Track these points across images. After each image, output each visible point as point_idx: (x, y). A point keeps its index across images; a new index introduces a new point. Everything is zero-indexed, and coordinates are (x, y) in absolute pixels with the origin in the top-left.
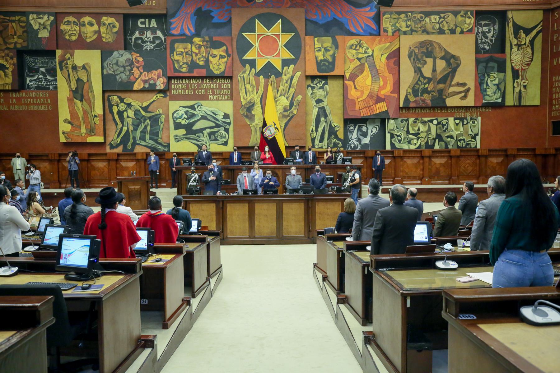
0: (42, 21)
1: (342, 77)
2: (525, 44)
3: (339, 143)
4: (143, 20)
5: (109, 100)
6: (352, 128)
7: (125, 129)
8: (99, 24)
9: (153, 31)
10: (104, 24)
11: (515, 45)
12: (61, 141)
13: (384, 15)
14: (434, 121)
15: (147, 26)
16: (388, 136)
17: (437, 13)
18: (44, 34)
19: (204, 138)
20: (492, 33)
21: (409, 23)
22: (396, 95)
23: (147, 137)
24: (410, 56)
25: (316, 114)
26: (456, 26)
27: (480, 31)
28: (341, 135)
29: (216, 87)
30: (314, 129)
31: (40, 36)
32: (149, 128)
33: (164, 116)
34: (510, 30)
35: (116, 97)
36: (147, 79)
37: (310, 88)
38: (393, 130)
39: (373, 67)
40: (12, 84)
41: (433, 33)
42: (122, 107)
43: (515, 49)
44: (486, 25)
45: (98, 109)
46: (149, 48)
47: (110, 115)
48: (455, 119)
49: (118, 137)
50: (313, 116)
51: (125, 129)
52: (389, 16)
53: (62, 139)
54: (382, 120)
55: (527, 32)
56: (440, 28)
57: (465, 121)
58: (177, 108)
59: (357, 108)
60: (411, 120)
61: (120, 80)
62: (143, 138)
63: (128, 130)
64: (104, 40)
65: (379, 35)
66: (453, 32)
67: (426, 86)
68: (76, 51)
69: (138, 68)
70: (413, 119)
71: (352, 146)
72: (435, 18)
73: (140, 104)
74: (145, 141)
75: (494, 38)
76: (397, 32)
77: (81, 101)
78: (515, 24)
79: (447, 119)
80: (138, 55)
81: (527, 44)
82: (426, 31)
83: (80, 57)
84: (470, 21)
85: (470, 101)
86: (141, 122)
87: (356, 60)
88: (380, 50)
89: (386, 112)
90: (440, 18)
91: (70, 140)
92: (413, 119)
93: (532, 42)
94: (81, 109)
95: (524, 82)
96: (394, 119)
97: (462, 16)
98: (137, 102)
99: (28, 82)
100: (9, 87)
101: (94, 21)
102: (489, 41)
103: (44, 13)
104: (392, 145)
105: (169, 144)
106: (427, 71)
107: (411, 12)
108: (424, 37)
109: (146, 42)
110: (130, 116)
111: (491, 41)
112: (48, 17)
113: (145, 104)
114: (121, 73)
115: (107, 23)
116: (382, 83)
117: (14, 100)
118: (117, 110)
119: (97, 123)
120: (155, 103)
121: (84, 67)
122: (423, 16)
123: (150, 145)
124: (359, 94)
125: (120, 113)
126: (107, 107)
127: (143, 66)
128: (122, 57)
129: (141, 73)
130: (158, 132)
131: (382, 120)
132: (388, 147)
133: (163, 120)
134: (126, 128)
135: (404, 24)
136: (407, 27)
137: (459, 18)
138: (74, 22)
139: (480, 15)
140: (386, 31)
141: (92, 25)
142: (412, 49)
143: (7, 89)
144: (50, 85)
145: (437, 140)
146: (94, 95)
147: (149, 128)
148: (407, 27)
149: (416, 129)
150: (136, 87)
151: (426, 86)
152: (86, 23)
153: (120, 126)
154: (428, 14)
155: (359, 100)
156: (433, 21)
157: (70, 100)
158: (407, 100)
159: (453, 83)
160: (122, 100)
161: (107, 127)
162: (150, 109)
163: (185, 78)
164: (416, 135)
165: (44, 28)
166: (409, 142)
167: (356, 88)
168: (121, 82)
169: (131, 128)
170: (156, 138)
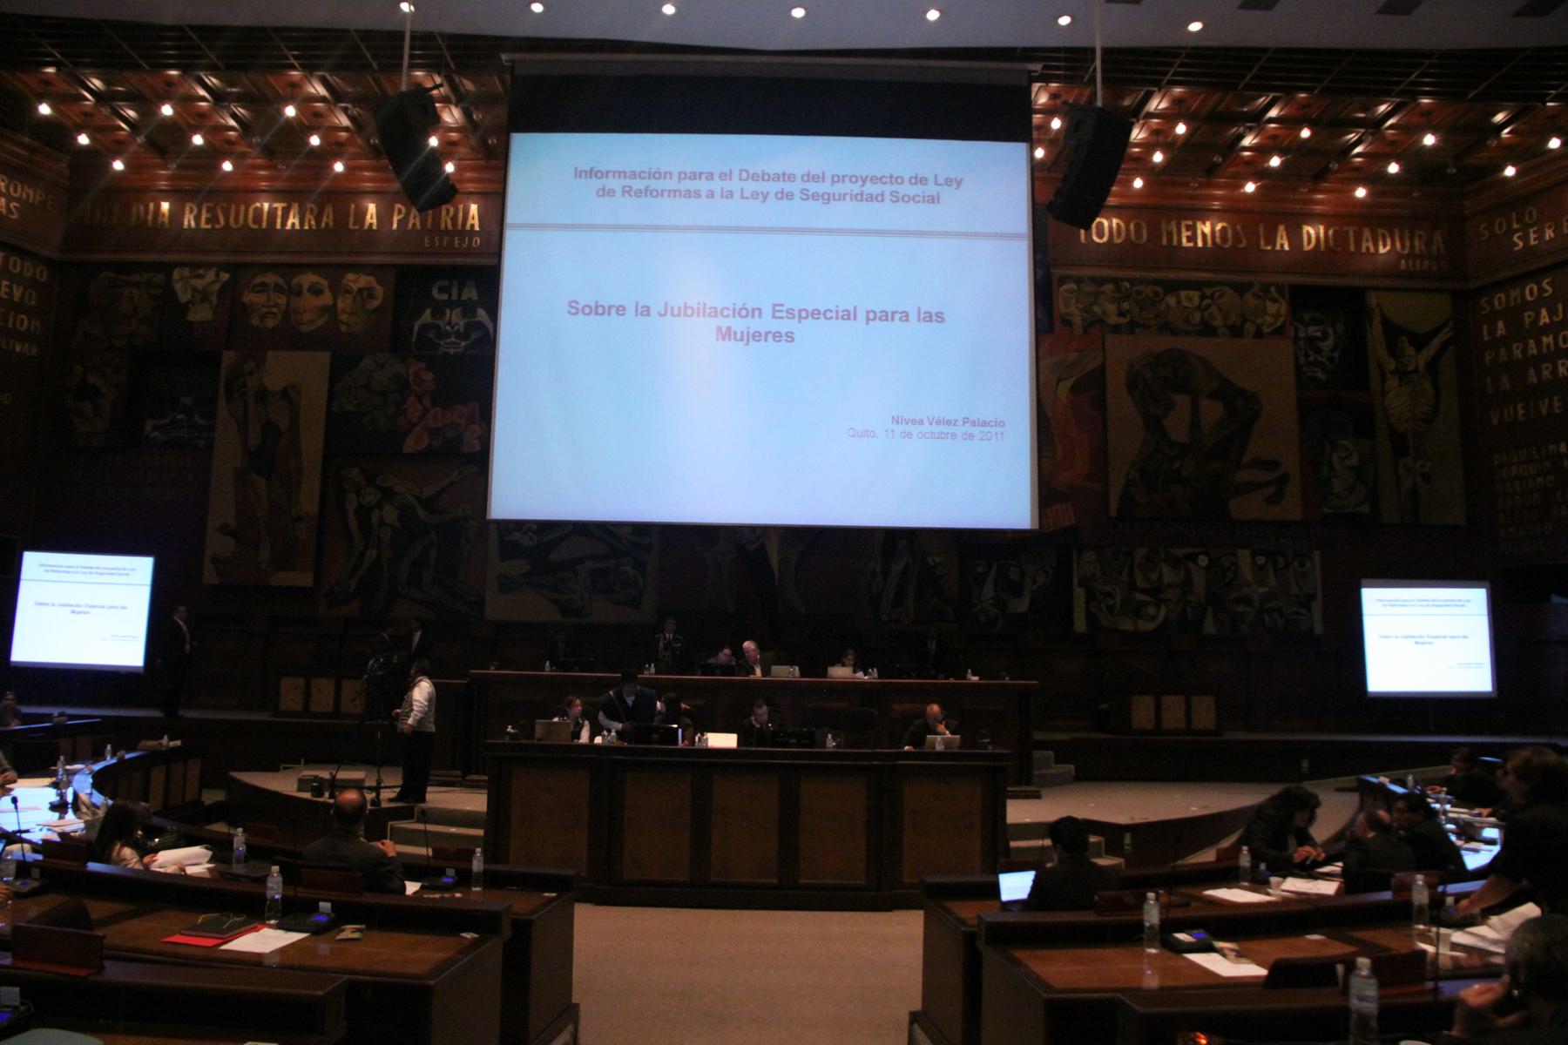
0: (199, 284)
2: (1416, 370)
4: (446, 283)
6: (980, 570)
7: (372, 554)
8: (337, 288)
9: (468, 309)
10: (348, 292)
11: (1393, 372)
13: (1063, 280)
14: (1201, 557)
15: (454, 297)
16: (1079, 593)
17: (1196, 285)
18: (201, 314)
20: (1330, 343)
21: (1126, 306)
26: (1245, 320)
27: (1302, 334)
30: (879, 569)
31: (191, 317)
34: (1375, 332)
35: (355, 471)
36: (440, 425)
41: (1188, 333)
42: (371, 497)
43: (1393, 382)
44: (1314, 322)
45: (309, 502)
46: (452, 351)
48: (1254, 554)
52: (1074, 286)
53: (210, 576)
55: (1420, 341)
56: (1203, 320)
57: (1280, 559)
60: (1140, 553)
64: (343, 328)
65: (1051, 330)
66: (1236, 331)
67: (1177, 465)
68: (270, 353)
69: (419, 397)
70: (1144, 550)
71: (983, 619)
72: (1191, 298)
75: (1336, 355)
76: (1095, 323)
78: (1386, 322)
79: (1235, 556)
80: (423, 365)
81: (1421, 369)
82: (1167, 328)
83: (279, 369)
84: (1277, 310)
85: (1291, 508)
90: (1203, 297)
92: (1144, 550)
93: (1432, 366)
95: (1423, 466)
97: (1257, 296)
101: (325, 283)
102: (1324, 360)
103: (208, 266)
104: (1091, 618)
106: (1177, 425)
107: (1131, 281)
108: (1166, 342)
109: (447, 335)
111: (1331, 359)
112: (217, 275)
113: (428, 492)
115: (355, 287)
121: (285, 393)
122: (1160, 290)
129: (426, 411)
132: (1080, 625)
134: (375, 552)
135: (1111, 308)
136: (1121, 314)
137: (1251, 301)
138: (276, 285)
139: (1301, 298)
140: (1067, 322)
141: (316, 291)
145: (1210, 609)
148: (1121, 314)
149: (1154, 576)
150: (409, 445)
151: (1177, 465)
152: (306, 287)
154: (1173, 287)
156: (1185, 303)
159: (1245, 459)
164: (1155, 591)
165: (204, 300)
166: (1137, 612)
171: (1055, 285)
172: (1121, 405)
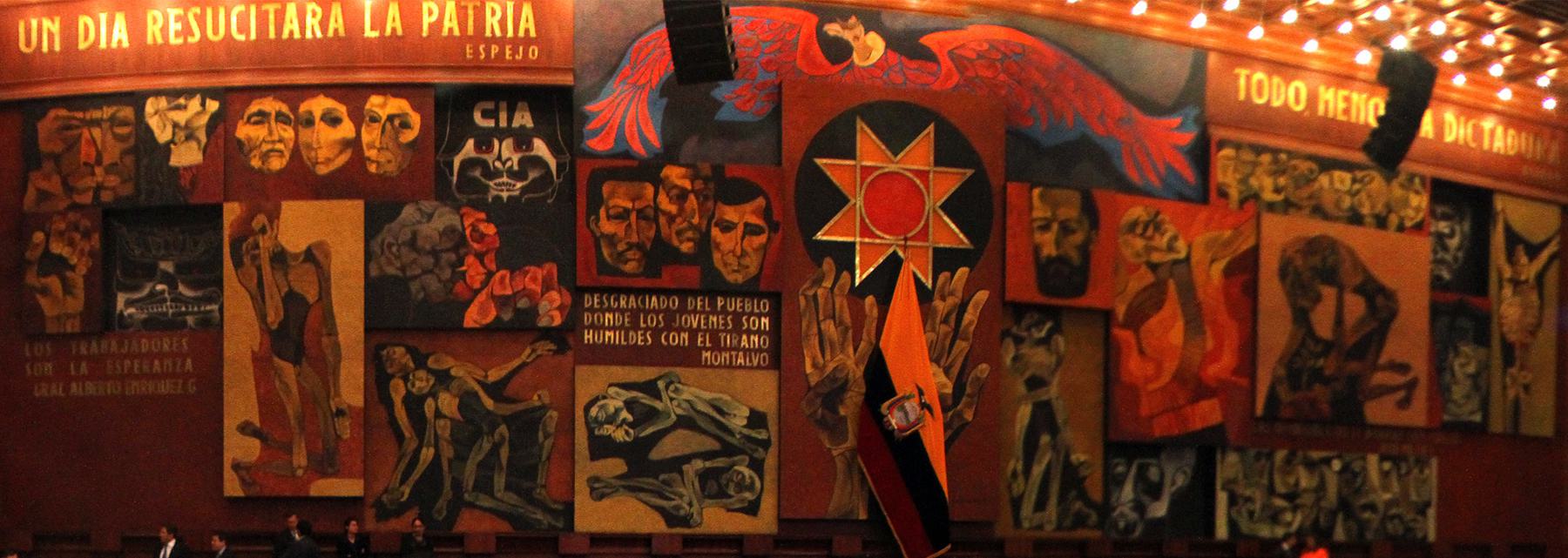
1: (1107, 315)
3: (1088, 516)
12: (226, 494)
19: (686, 494)
21: (1282, 181)
22: (1244, 382)
23: (500, 481)
24: (1283, 273)
25: (1026, 421)
28: (1096, 495)
29: (726, 324)
32: (504, 452)
33: (555, 414)
37: (1009, 342)
38: (1234, 481)
39: (1188, 292)
42: (422, 382)
47: (382, 408)
49: (402, 482)
50: (1018, 427)
51: (427, 454)
54: (1207, 447)
58: (603, 392)
59: (1145, 411)
61: (421, 295)
62: (484, 485)
63: (437, 456)
73: (479, 374)
74: (492, 496)
76: (1251, 197)
77: (296, 362)
86: (477, 435)
87: (1144, 268)
88: (1209, 245)
89: (1218, 429)
94: (295, 390)
96: (1239, 449)
98: (470, 367)
105: (569, 510)
107: (1289, 153)
110: (445, 411)
113: (494, 375)
114: (425, 272)
116: (1210, 344)
118: (403, 392)
120: (527, 372)
123: (503, 507)
124: (1150, 369)
125: (414, 403)
127: (498, 251)
128: (432, 221)
130: (534, 468)
131: (1207, 447)
133: (551, 429)
134: (432, 450)
135: (1268, 182)
136: (1277, 190)
140: (1223, 194)
142: (1290, 252)
146: (337, 345)
147: (504, 452)
148: (1277, 190)
155: (1152, 387)
158: (1272, 397)
160: (420, 363)
162: (509, 391)
163: (628, 291)
167: (1141, 352)
168: (425, 300)
169: (448, 452)
170: (526, 484)
171: (1213, 148)
172: (1272, 292)
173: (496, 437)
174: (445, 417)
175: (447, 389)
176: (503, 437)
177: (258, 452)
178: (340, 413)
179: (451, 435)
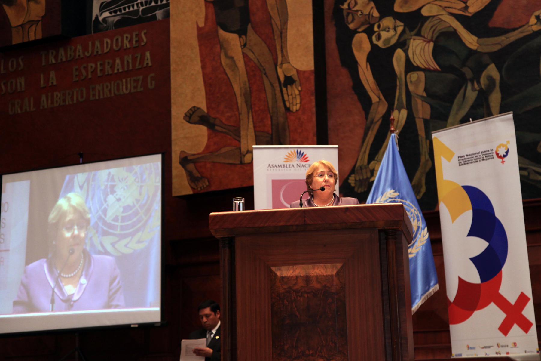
5: (339, 17)
40: (45, 20)
42: (389, 32)
45: (299, 54)
47: (344, 72)
63: (411, 119)
77: (242, 32)
91: (203, 186)
94: (241, 64)
99: (96, 11)
100: (35, 34)
110: (417, 61)
117: (52, 74)
118: (367, 47)
119: (295, 108)
125: (380, 59)
126: (331, 45)
134: (404, 113)
143: (32, 38)
144: (155, 9)
153: (379, 109)
157: (207, 39)
161: (331, 123)
162: (498, 19)
169: (423, 111)
173: (483, 80)
174: (417, 69)
175: (419, 34)
176: (491, 79)
177: (205, 141)
178: (289, 81)
179: (426, 90)
